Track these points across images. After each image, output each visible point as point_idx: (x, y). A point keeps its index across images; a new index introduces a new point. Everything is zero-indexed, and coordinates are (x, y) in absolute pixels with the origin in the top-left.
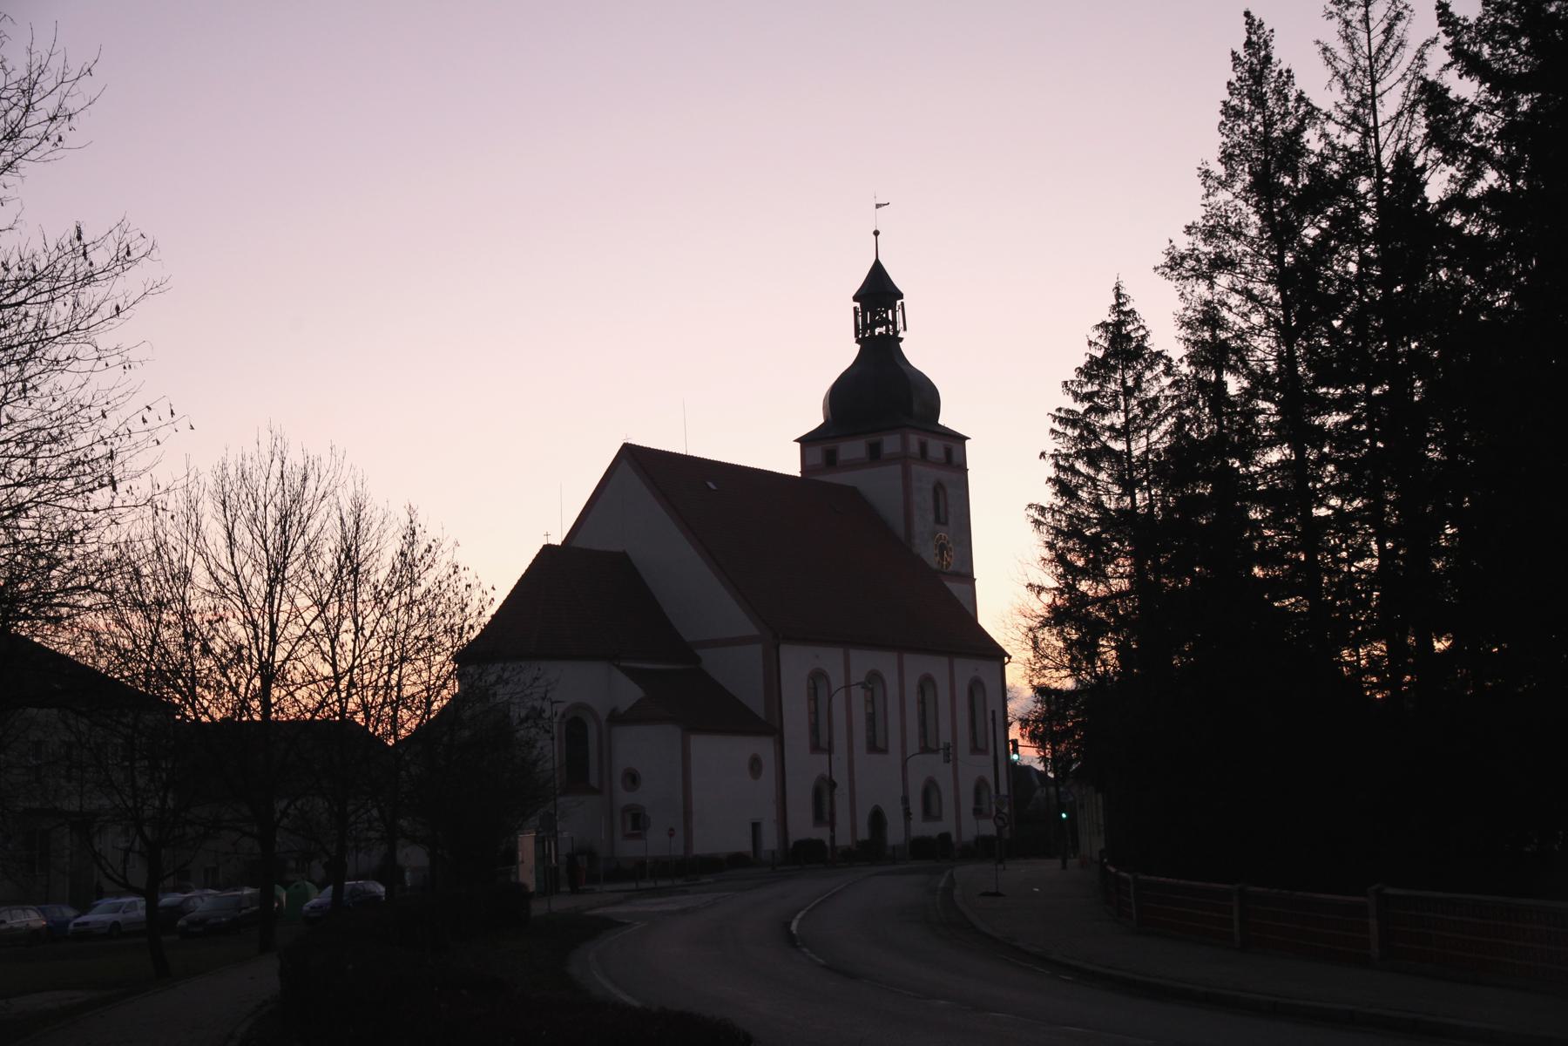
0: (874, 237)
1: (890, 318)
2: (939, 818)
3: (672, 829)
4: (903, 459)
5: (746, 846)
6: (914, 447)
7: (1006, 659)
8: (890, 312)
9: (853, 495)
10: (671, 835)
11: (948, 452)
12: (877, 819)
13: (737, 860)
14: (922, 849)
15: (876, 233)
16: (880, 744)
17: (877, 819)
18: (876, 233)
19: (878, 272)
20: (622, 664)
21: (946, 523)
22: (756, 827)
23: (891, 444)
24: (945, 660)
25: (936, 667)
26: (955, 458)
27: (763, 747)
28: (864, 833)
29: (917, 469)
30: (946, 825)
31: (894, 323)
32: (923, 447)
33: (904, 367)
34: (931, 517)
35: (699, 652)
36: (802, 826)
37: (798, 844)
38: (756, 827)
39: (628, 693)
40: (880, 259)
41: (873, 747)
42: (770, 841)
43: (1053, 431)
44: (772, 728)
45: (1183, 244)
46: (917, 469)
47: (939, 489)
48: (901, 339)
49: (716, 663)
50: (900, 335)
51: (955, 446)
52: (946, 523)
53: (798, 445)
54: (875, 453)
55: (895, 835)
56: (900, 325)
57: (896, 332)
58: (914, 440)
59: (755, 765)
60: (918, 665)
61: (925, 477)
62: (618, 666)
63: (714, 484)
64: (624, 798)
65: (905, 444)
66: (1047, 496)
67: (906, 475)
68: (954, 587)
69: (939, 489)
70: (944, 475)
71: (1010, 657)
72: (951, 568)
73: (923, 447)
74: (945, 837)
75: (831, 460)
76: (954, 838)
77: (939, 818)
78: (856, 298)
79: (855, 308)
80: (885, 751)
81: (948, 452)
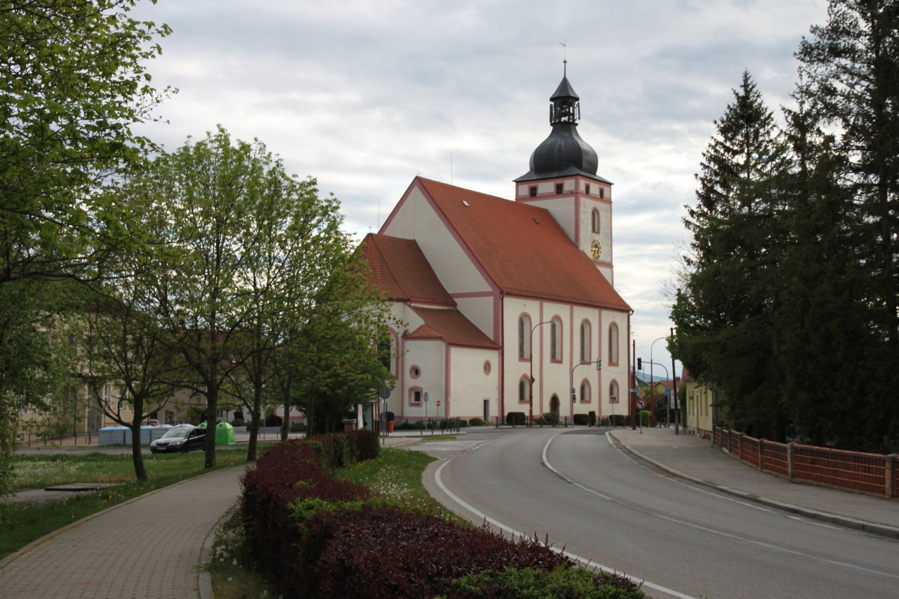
1: (571, 111)
2: (589, 402)
3: (439, 402)
4: (574, 193)
5: (479, 414)
6: (582, 188)
7: (631, 312)
8: (571, 108)
9: (545, 213)
10: (438, 405)
11: (602, 192)
12: (555, 401)
13: (475, 422)
14: (579, 420)
15: (565, 62)
16: (558, 357)
17: (555, 401)
18: (565, 62)
19: (565, 84)
20: (412, 305)
21: (598, 233)
22: (486, 402)
23: (569, 184)
24: (596, 311)
25: (591, 314)
26: (606, 195)
27: (492, 356)
28: (547, 409)
29: (583, 200)
30: (593, 407)
31: (573, 115)
32: (587, 188)
33: (579, 142)
34: (590, 228)
35: (456, 300)
36: (513, 405)
37: (511, 415)
38: (486, 402)
39: (415, 322)
40: (567, 76)
41: (554, 359)
42: (494, 412)
43: (702, 164)
44: (497, 345)
45: (812, 39)
46: (583, 200)
47: (595, 212)
48: (577, 125)
49: (464, 306)
50: (576, 122)
51: (606, 189)
52: (598, 233)
53: (515, 183)
54: (559, 189)
55: (564, 411)
56: (576, 116)
57: (574, 120)
58: (582, 183)
59: (487, 367)
60: (582, 313)
61: (587, 205)
62: (409, 306)
63: (467, 202)
64: (410, 382)
65: (577, 185)
66: (695, 203)
67: (577, 204)
68: (603, 270)
69: (595, 212)
70: (600, 205)
71: (633, 311)
72: (600, 259)
73: (587, 188)
74: (592, 414)
75: (533, 192)
76: (597, 414)
77: (589, 402)
78: (552, 100)
79: (551, 105)
80: (560, 362)
81: (602, 192)
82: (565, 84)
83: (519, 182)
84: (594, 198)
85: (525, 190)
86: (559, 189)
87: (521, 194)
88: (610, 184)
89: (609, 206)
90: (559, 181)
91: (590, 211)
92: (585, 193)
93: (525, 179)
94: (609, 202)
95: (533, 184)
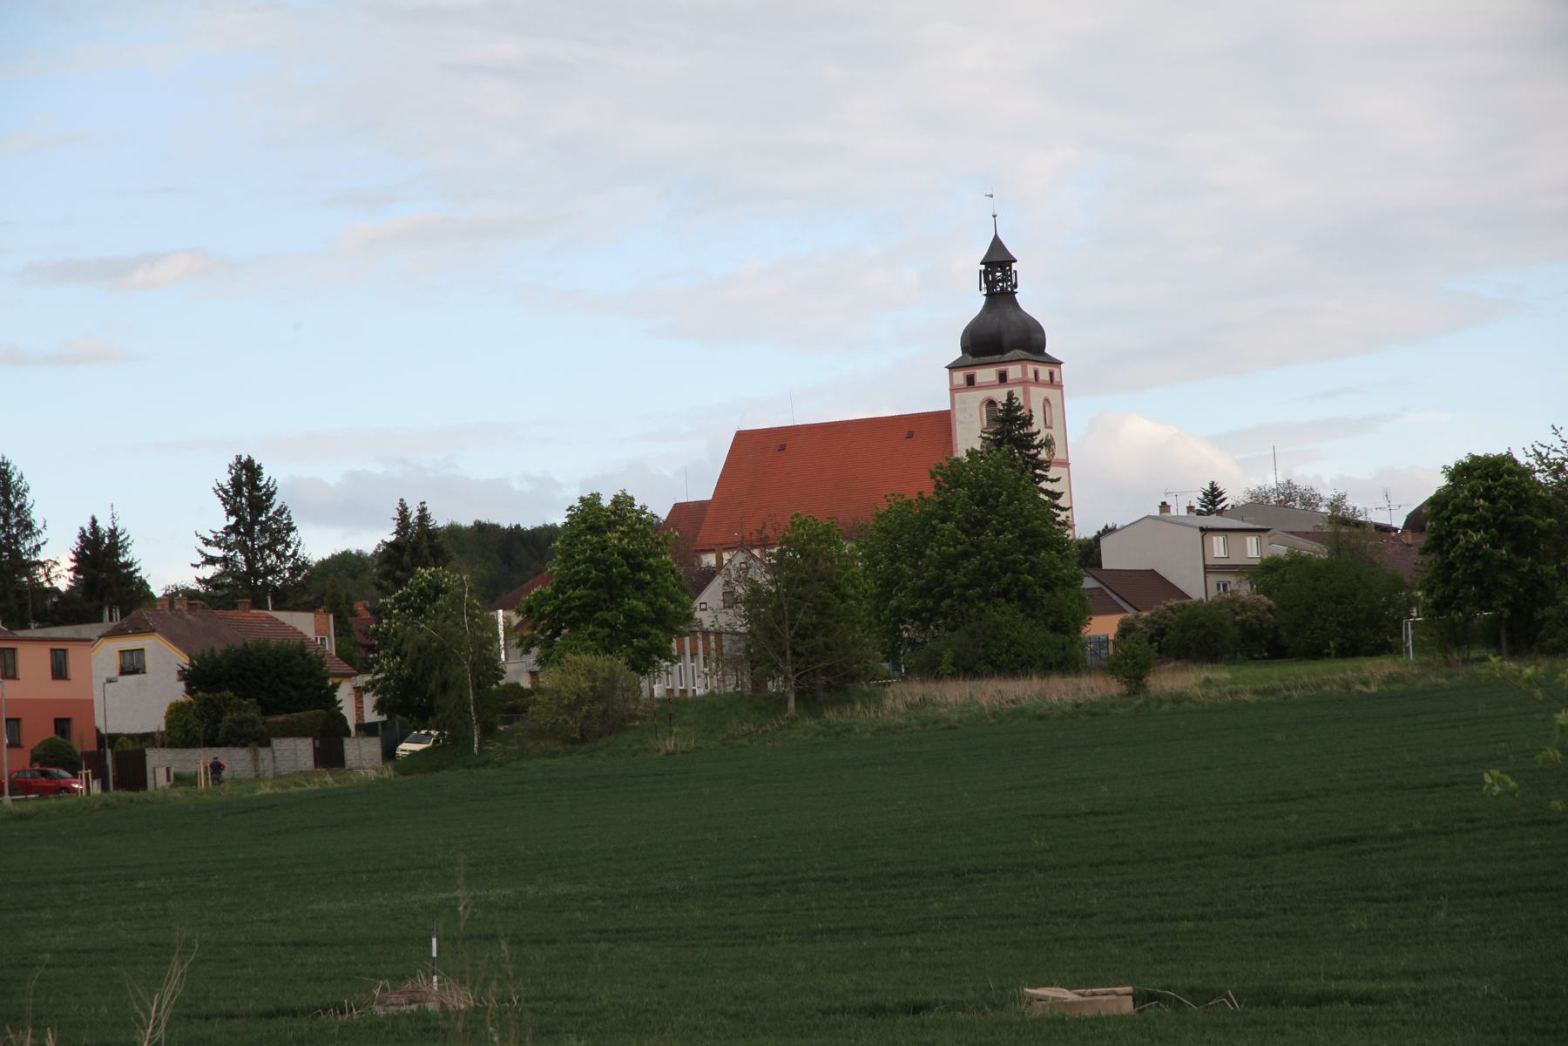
6: (1031, 375)
11: (1051, 374)
15: (995, 216)
18: (995, 216)
19: (997, 245)
26: (1056, 378)
32: (1036, 373)
46: (1033, 390)
51: (1056, 370)
53: (947, 370)
54: (1003, 377)
58: (1031, 368)
65: (1024, 372)
73: (1036, 373)
78: (982, 263)
81: (1051, 374)
82: (997, 245)
83: (952, 368)
84: (1044, 385)
85: (960, 377)
86: (1003, 377)
87: (955, 383)
88: (1060, 363)
89: (1060, 391)
90: (1002, 368)
91: (1042, 400)
92: (1034, 381)
94: (1060, 386)
95: (970, 371)
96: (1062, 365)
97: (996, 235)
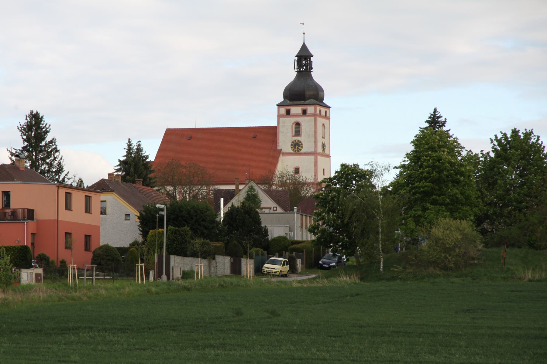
0: (303, 35)
4: (314, 115)
6: (318, 112)
15: (304, 34)
18: (304, 34)
19: (304, 48)
23: (310, 109)
26: (328, 115)
29: (319, 119)
32: (320, 111)
46: (319, 119)
51: (328, 111)
53: (277, 106)
54: (304, 112)
67: (315, 121)
73: (320, 111)
82: (304, 48)
83: (279, 105)
86: (304, 112)
87: (280, 113)
90: (304, 107)
93: (280, 105)
95: (288, 108)
96: (330, 108)
97: (304, 43)
